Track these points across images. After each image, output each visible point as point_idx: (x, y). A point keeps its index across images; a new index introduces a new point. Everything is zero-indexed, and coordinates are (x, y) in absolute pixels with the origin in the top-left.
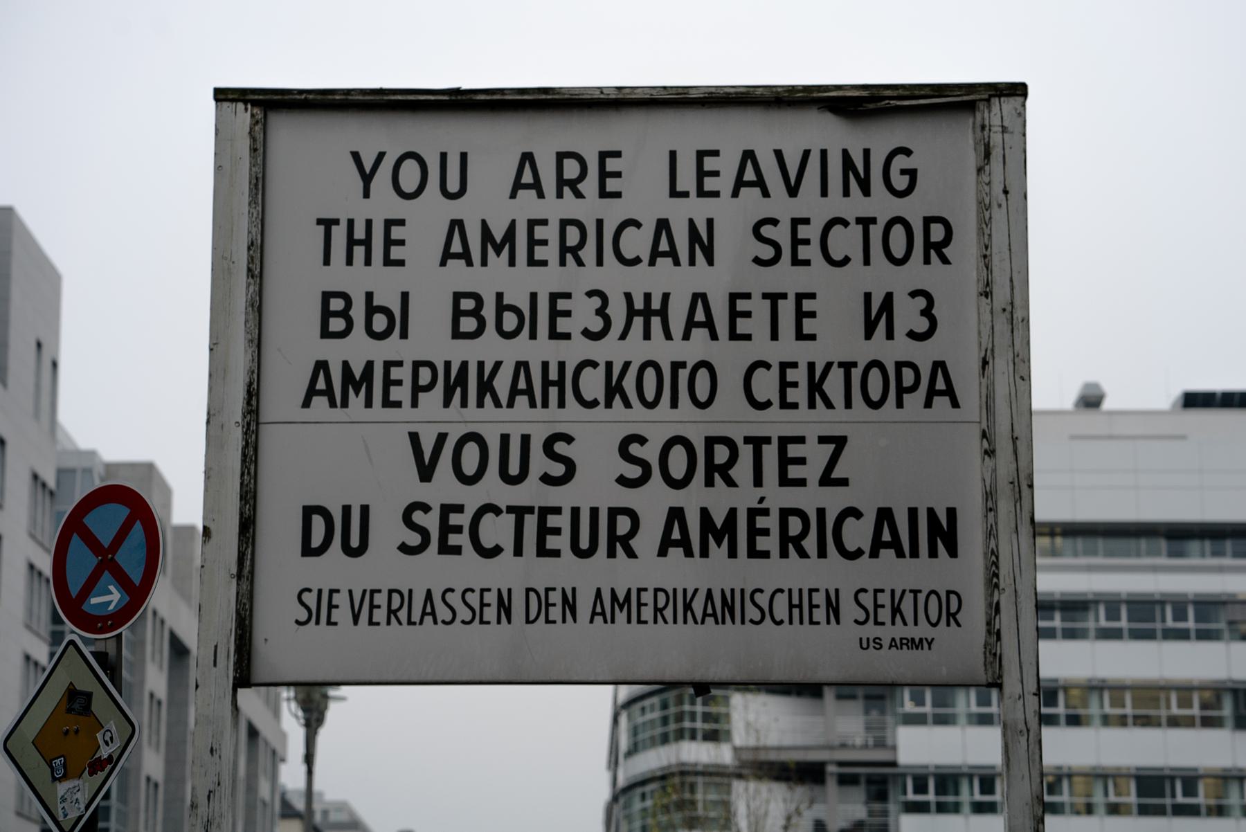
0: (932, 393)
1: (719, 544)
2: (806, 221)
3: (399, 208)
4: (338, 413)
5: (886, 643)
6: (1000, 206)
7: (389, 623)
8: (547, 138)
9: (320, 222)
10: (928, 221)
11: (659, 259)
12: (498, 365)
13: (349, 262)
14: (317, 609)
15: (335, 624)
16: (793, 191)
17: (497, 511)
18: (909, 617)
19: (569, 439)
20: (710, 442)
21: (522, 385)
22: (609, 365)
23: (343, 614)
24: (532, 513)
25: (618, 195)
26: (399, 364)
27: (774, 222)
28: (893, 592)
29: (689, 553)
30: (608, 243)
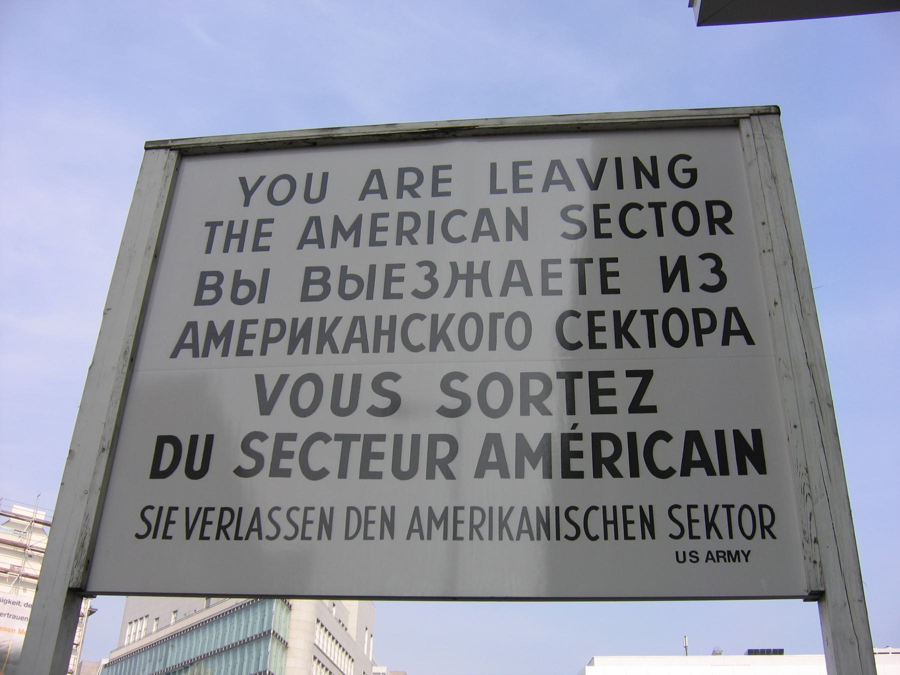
1: (534, 466)
2: (607, 206)
3: (270, 211)
4: (200, 359)
5: (702, 556)
6: (770, 188)
7: (218, 538)
9: (207, 224)
10: (710, 205)
11: (480, 237)
12: (337, 320)
13: (226, 249)
14: (156, 525)
15: (170, 538)
17: (324, 437)
18: (724, 531)
19: (395, 377)
20: (526, 378)
21: (357, 334)
22: (435, 318)
23: (178, 530)
24: (359, 440)
26: (255, 322)
28: (706, 507)
29: (505, 474)
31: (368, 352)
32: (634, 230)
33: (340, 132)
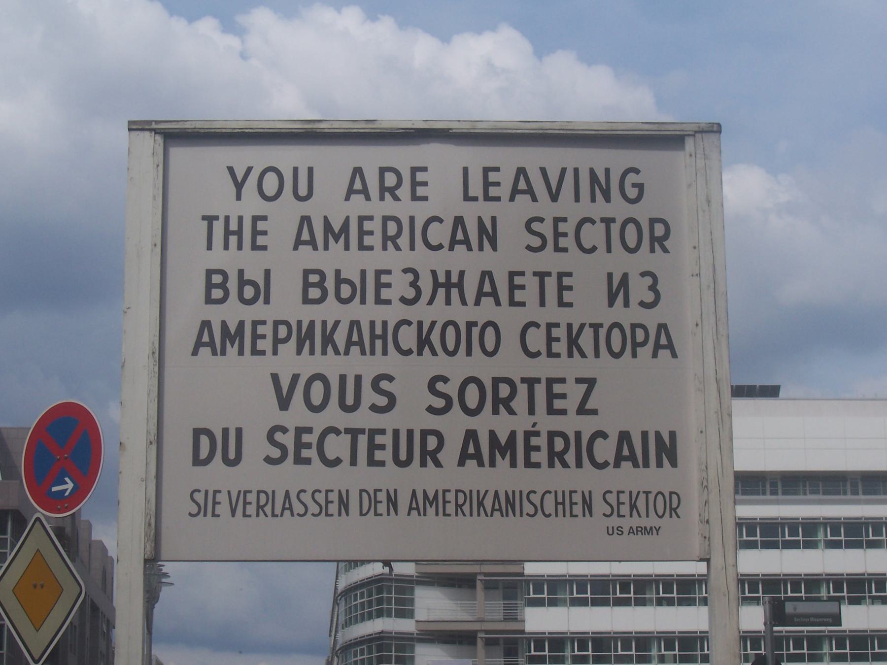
0: (657, 347)
2: (565, 220)
4: (219, 357)
5: (626, 530)
6: (704, 211)
7: (258, 515)
8: (371, 158)
9: (204, 218)
10: (653, 221)
11: (456, 246)
12: (337, 323)
13: (226, 247)
14: (205, 505)
15: (218, 516)
16: (554, 197)
17: (337, 432)
18: (643, 511)
19: (390, 379)
20: (496, 381)
21: (355, 338)
22: (420, 324)
23: (223, 509)
25: (425, 199)
26: (264, 323)
27: (541, 220)
28: (631, 492)
29: (481, 464)
30: (420, 234)
31: (365, 354)
32: (587, 245)
33: (322, 126)
